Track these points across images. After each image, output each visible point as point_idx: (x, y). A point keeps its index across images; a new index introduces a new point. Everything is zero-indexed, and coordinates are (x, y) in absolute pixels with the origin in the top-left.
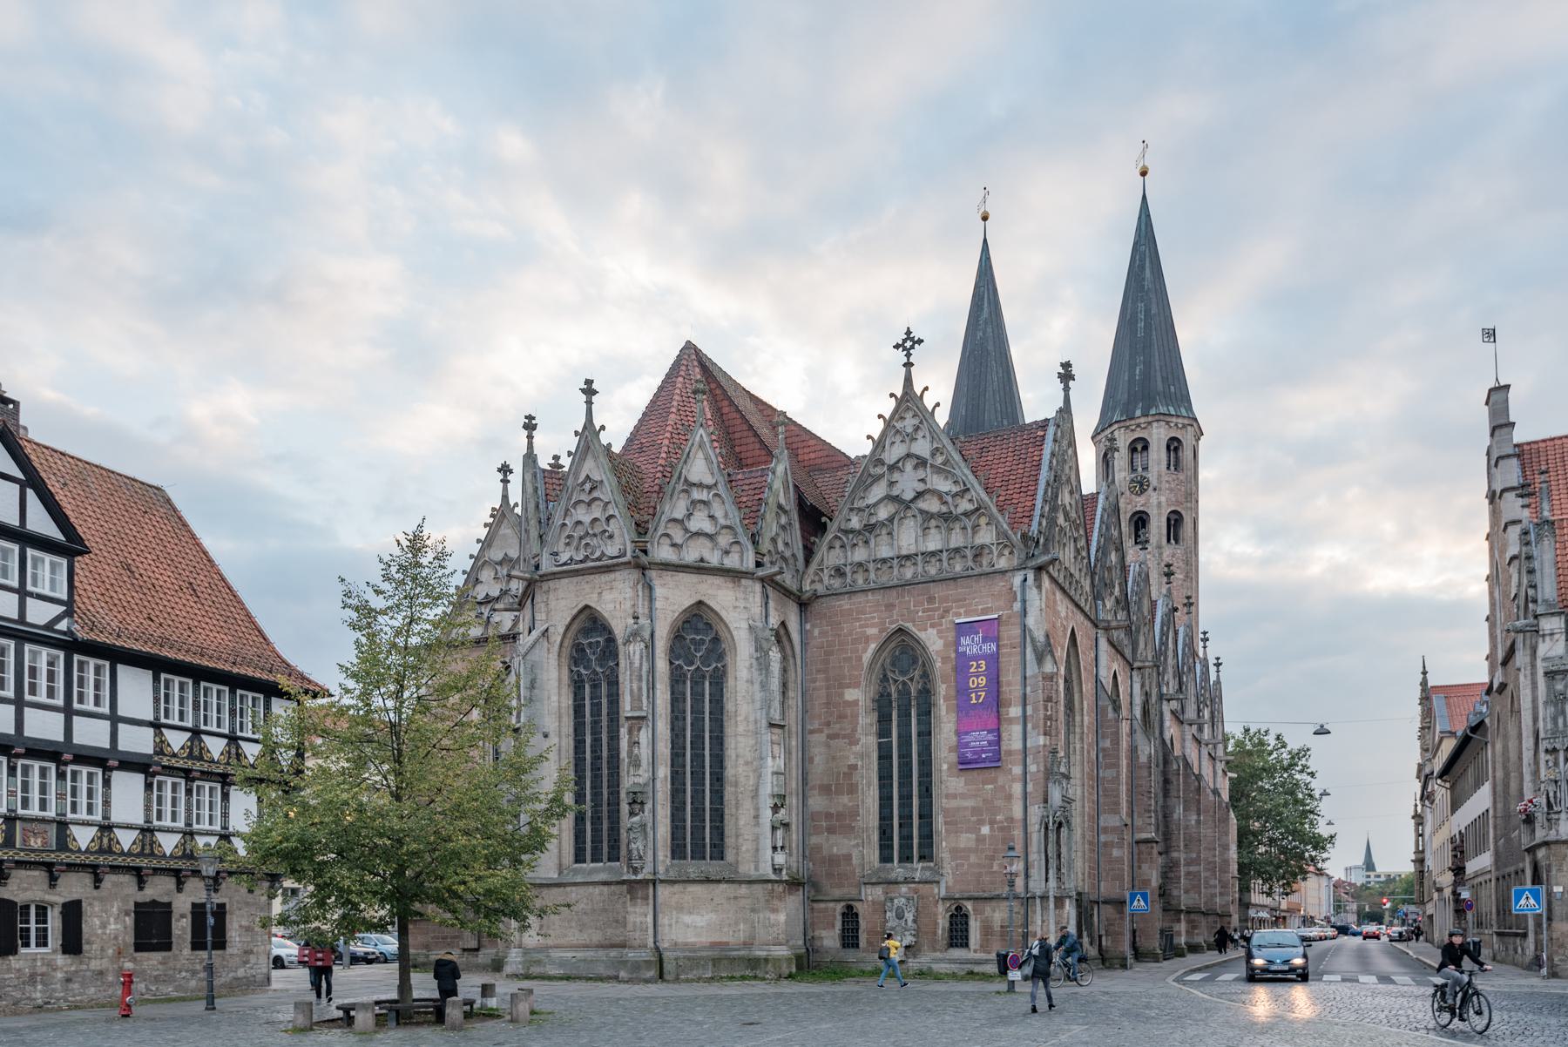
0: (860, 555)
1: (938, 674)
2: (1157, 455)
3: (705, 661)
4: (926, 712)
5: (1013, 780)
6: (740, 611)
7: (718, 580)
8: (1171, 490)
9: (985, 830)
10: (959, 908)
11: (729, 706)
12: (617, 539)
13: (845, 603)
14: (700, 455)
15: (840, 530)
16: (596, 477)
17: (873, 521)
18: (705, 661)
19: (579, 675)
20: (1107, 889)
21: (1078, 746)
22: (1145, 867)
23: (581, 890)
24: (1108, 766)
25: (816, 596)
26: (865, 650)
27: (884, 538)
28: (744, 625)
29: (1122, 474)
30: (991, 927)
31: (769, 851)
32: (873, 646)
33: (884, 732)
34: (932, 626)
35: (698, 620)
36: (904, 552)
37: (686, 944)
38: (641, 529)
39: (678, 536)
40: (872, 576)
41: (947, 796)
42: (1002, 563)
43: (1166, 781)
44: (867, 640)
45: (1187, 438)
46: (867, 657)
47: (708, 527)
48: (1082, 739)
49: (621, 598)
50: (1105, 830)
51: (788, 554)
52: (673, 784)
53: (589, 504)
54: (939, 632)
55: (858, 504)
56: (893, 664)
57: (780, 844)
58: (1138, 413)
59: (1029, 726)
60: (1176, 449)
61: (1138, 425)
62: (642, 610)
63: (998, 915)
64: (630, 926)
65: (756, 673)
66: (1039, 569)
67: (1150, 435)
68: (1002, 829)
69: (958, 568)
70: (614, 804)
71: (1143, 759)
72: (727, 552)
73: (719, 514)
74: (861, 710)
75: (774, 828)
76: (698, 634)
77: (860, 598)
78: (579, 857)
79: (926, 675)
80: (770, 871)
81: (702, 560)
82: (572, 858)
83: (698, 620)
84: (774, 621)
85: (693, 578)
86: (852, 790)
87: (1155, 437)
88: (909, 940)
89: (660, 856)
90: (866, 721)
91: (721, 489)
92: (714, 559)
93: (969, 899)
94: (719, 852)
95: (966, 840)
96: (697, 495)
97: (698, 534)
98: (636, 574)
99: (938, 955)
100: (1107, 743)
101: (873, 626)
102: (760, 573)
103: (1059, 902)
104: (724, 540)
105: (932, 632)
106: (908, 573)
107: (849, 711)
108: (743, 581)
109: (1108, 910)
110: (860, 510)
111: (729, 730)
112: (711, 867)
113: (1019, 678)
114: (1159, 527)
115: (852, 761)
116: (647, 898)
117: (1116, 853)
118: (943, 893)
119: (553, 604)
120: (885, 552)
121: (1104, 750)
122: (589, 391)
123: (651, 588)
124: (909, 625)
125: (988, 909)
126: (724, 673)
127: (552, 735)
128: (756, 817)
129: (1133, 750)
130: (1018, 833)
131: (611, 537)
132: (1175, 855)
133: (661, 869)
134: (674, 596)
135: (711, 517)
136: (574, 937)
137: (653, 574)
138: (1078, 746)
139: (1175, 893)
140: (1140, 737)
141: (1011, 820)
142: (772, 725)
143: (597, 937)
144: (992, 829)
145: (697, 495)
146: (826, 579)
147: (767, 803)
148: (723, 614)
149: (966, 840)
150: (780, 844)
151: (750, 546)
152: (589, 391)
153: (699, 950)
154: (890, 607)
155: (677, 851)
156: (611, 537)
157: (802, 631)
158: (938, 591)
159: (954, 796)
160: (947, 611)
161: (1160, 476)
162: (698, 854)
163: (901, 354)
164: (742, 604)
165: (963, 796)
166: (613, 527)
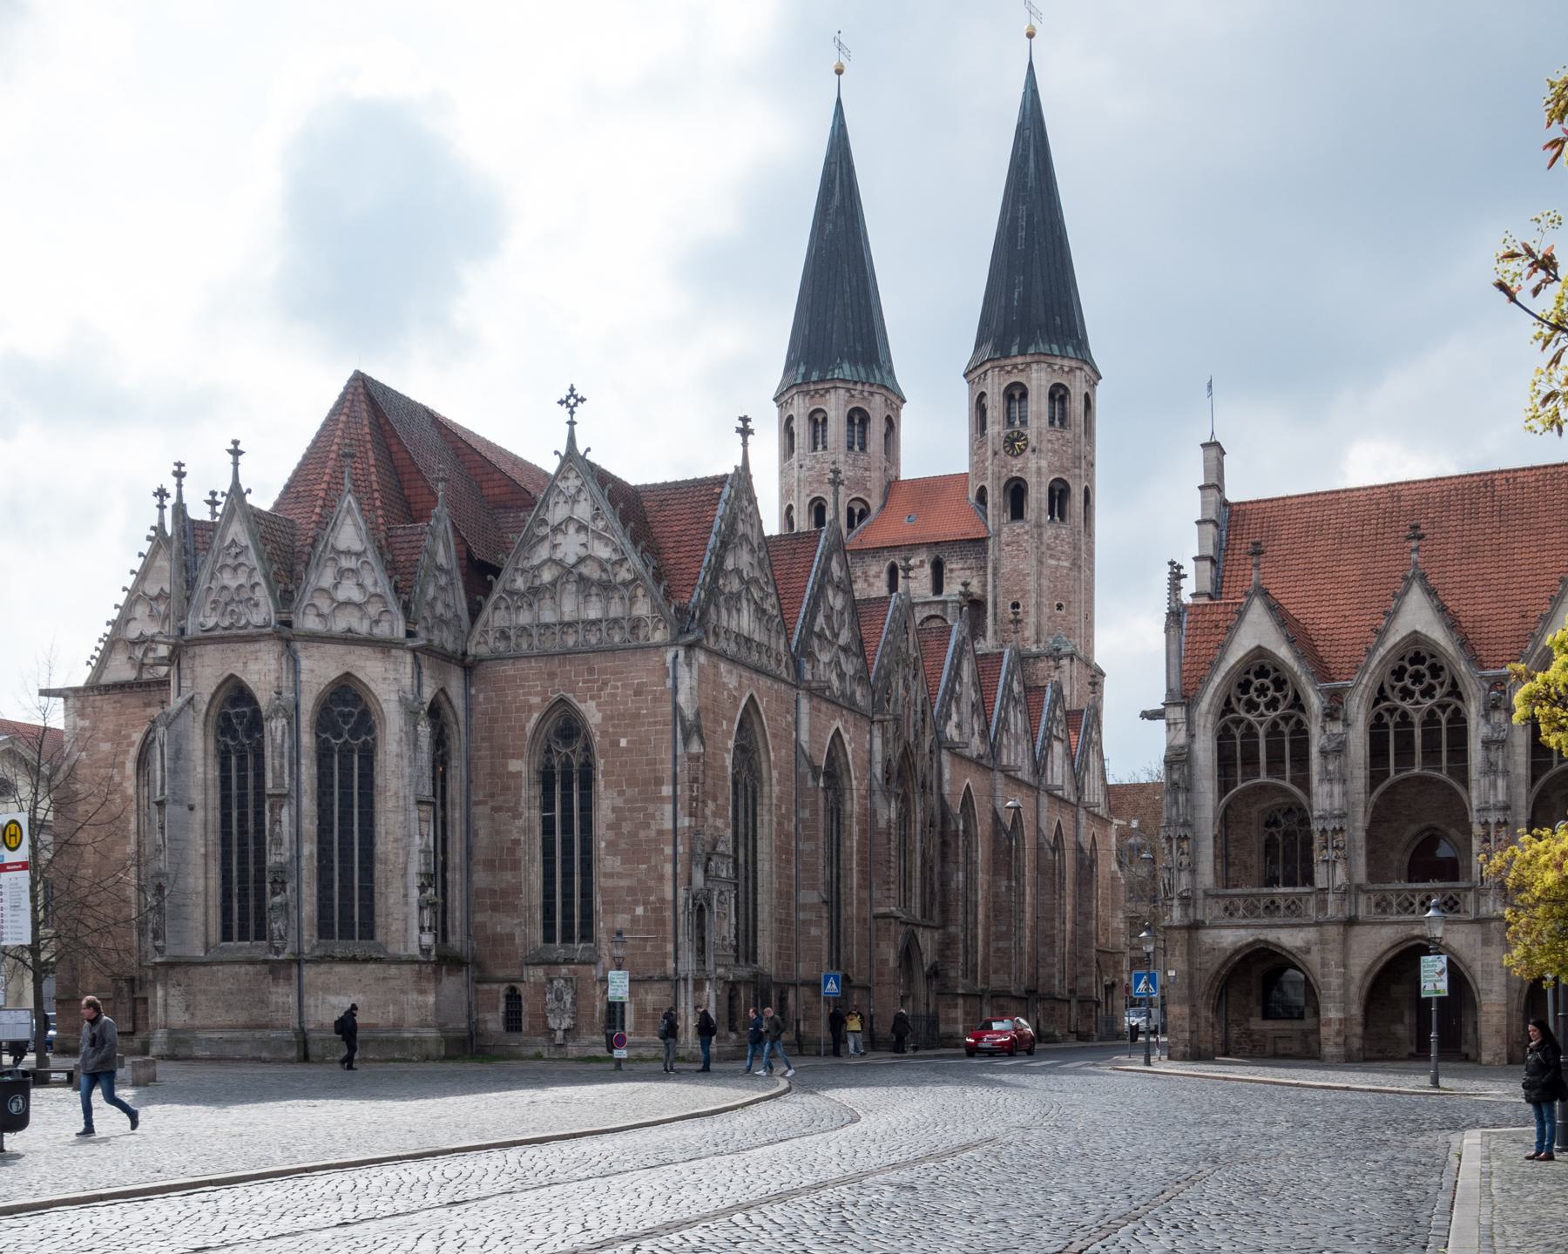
2: (1038, 405)
3: (354, 734)
5: (665, 861)
6: (389, 683)
7: (366, 651)
8: (1055, 452)
9: (639, 911)
11: (379, 781)
12: (263, 609)
13: (509, 669)
14: (349, 521)
15: (505, 590)
17: (537, 583)
18: (354, 734)
19: (226, 745)
20: (804, 970)
21: (766, 818)
22: (883, 944)
23: (227, 969)
24: (809, 838)
25: (479, 660)
26: (528, 720)
27: (547, 603)
28: (394, 697)
31: (417, 932)
32: (536, 715)
33: (548, 805)
34: (592, 698)
36: (567, 618)
38: (286, 598)
39: (324, 605)
40: (536, 642)
41: (606, 875)
43: (945, 844)
44: (531, 708)
45: (1077, 388)
46: (530, 726)
47: (357, 596)
48: (770, 811)
50: (804, 907)
51: (449, 615)
52: (319, 861)
53: (235, 569)
54: (598, 705)
55: (526, 564)
57: (427, 924)
58: (1015, 350)
60: (1063, 399)
61: (1015, 366)
62: (287, 682)
64: (273, 1008)
65: (405, 748)
66: (690, 647)
68: (655, 910)
70: (260, 880)
71: (882, 824)
72: (377, 622)
73: (368, 582)
74: (524, 783)
75: (421, 909)
76: (346, 707)
77: (523, 664)
78: (226, 935)
79: (588, 748)
80: (416, 951)
81: (350, 630)
82: (219, 936)
84: (428, 693)
85: (341, 649)
86: (515, 866)
87: (1034, 383)
89: (305, 935)
90: (529, 794)
91: (370, 557)
92: (363, 628)
94: (368, 931)
96: (346, 563)
97: (348, 603)
100: (806, 814)
101: (536, 694)
102: (411, 643)
103: (699, 986)
104: (374, 609)
105: (592, 704)
107: (512, 783)
108: (394, 652)
109: (805, 992)
110: (524, 571)
111: (379, 806)
112: (357, 947)
114: (1039, 500)
115: (515, 836)
116: (289, 978)
117: (814, 931)
120: (548, 617)
121: (804, 820)
122: (236, 453)
123: (296, 661)
124: (570, 695)
126: (375, 745)
127: (197, 807)
128: (406, 896)
129: (870, 815)
130: (669, 914)
131: (256, 605)
132: (952, 929)
133: (306, 949)
135: (360, 585)
136: (222, 1018)
137: (298, 645)
138: (766, 818)
139: (952, 973)
140: (879, 799)
141: (662, 900)
142: (419, 802)
143: (242, 1017)
145: (346, 563)
146: (491, 641)
147: (414, 882)
148: (372, 686)
149: (622, 921)
150: (427, 924)
151: (401, 616)
152: (236, 453)
154: (552, 675)
155: (324, 930)
157: (468, 697)
158: (598, 662)
160: (605, 684)
161: (1040, 433)
162: (347, 933)
163: (565, 410)
164: (391, 675)
165: (620, 876)
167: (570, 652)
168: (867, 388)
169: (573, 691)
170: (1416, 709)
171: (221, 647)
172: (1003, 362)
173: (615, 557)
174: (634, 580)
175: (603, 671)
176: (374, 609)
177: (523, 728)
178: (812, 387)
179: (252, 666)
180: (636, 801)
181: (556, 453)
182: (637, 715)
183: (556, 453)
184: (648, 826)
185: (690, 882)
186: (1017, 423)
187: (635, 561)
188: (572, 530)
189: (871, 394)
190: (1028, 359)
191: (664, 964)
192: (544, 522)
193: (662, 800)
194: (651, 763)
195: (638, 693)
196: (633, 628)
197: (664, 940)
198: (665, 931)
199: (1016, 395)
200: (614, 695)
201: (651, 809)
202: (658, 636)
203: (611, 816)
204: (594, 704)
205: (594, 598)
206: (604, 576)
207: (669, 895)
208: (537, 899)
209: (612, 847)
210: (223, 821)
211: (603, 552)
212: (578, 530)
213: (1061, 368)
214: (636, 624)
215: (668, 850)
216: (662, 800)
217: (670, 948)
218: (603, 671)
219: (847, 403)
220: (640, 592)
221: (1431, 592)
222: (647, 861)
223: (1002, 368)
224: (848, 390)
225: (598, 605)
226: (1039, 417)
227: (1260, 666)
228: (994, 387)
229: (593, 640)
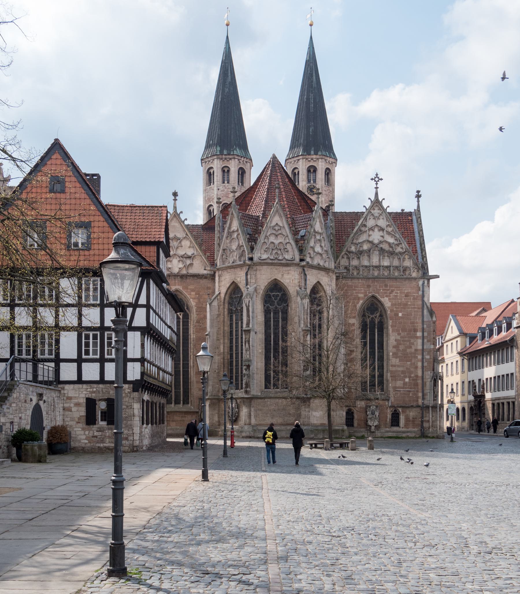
0: (355, 262)
1: (388, 316)
2: (320, 175)
5: (418, 361)
7: (323, 273)
10: (395, 411)
13: (349, 282)
15: (347, 251)
16: (280, 224)
17: (361, 249)
23: (273, 401)
26: (358, 303)
30: (409, 418)
32: (361, 302)
33: (364, 337)
34: (386, 296)
36: (374, 264)
37: (314, 424)
40: (361, 273)
41: (392, 366)
44: (359, 299)
47: (320, 251)
49: (293, 278)
53: (277, 236)
54: (389, 299)
55: (354, 241)
56: (367, 309)
58: (312, 152)
59: (425, 340)
61: (312, 159)
63: (412, 413)
67: (318, 164)
68: (413, 380)
69: (396, 274)
73: (323, 245)
76: (315, 294)
77: (356, 281)
79: (381, 316)
83: (316, 289)
87: (320, 166)
88: (376, 423)
91: (324, 235)
93: (400, 407)
95: (399, 383)
97: (318, 253)
99: (387, 429)
101: (362, 293)
105: (386, 299)
106: (376, 273)
110: (356, 244)
113: (421, 321)
118: (390, 405)
120: (366, 263)
124: (377, 295)
125: (408, 411)
130: (420, 382)
131: (287, 251)
135: (321, 246)
141: (417, 376)
144: (409, 380)
145: (318, 237)
148: (325, 287)
149: (399, 383)
153: (317, 426)
154: (369, 286)
156: (287, 251)
158: (389, 283)
159: (395, 366)
160: (392, 291)
165: (398, 366)
166: (288, 247)
167: (377, 278)
168: (245, 159)
169: (378, 293)
171: (270, 267)
172: (307, 157)
173: (396, 242)
174: (405, 252)
175: (391, 286)
176: (324, 256)
177: (356, 307)
178: (224, 157)
180: (406, 338)
181: (369, 199)
182: (406, 304)
183: (369, 199)
184: (411, 347)
185: (433, 370)
186: (312, 182)
187: (405, 245)
188: (376, 230)
189: (246, 162)
190: (318, 157)
191: (417, 401)
192: (365, 226)
193: (417, 338)
194: (413, 323)
195: (407, 296)
196: (404, 271)
197: (418, 391)
198: (418, 388)
199: (312, 170)
200: (396, 296)
201: (412, 341)
202: (414, 275)
203: (395, 343)
204: (387, 299)
205: (386, 257)
206: (391, 249)
209: (395, 355)
210: (266, 339)
211: (391, 240)
212: (379, 231)
213: (329, 162)
214: (405, 269)
215: (420, 357)
216: (417, 338)
217: (420, 394)
218: (391, 286)
219: (238, 165)
220: (407, 257)
222: (410, 361)
223: (307, 159)
224: (239, 160)
225: (388, 260)
226: (322, 181)
229: (386, 274)
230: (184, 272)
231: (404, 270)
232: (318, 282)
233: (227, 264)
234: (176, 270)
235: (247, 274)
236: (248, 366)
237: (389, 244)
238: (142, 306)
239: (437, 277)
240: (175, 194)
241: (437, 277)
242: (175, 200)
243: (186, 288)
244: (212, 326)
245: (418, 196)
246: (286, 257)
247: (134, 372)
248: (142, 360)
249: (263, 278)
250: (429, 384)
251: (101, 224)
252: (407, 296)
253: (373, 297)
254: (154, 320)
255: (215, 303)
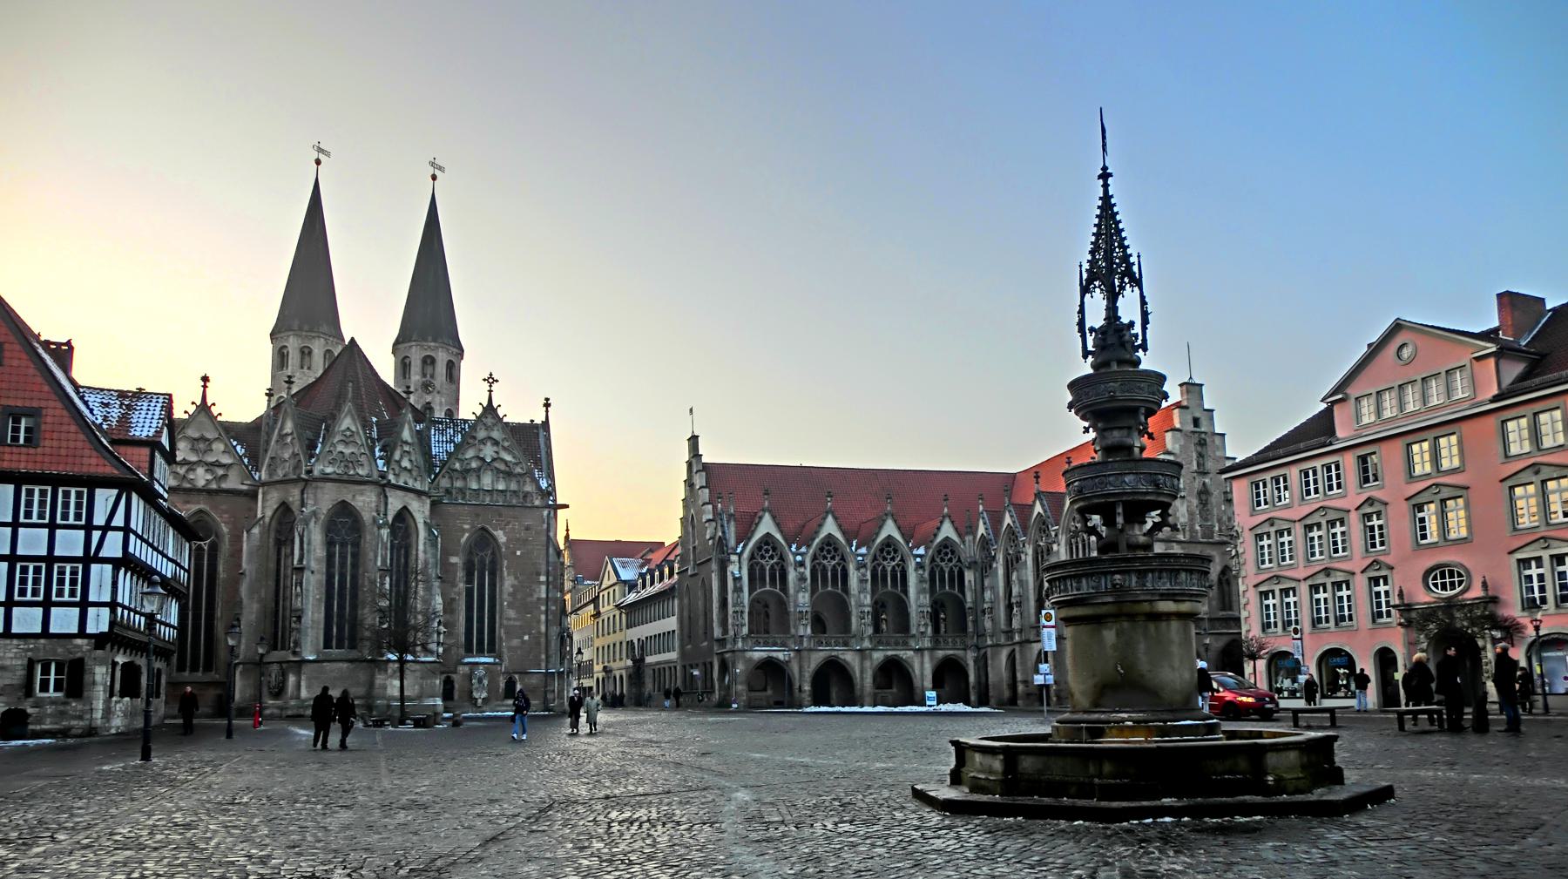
4: (493, 575)
6: (420, 511)
13: (451, 509)
29: (416, 378)
33: (469, 580)
35: (404, 514)
42: (537, 503)
44: (464, 531)
46: (463, 540)
83: (404, 514)
90: (460, 574)
92: (411, 484)
96: (407, 448)
98: (379, 490)
119: (319, 495)
120: (474, 486)
134: (395, 502)
145: (407, 448)
170: (829, 564)
179: (359, 498)
199: (429, 361)
207: (543, 628)
208: (462, 629)
211: (508, 458)
221: (836, 518)
227: (768, 539)
228: (416, 356)
230: (214, 486)
231: (525, 497)
232: (405, 508)
233: (276, 478)
234: (201, 483)
235: (302, 493)
236: (299, 618)
237: (506, 462)
238: (117, 529)
239: (566, 506)
240: (205, 379)
241: (566, 506)
242: (205, 387)
243: (214, 508)
244: (249, 562)
245: (547, 405)
246: (360, 472)
247: (99, 622)
248: (113, 605)
249: (324, 500)
250: (554, 644)
251: (57, 412)
252: (527, 528)
253: (483, 529)
254: (135, 547)
255: (256, 530)
